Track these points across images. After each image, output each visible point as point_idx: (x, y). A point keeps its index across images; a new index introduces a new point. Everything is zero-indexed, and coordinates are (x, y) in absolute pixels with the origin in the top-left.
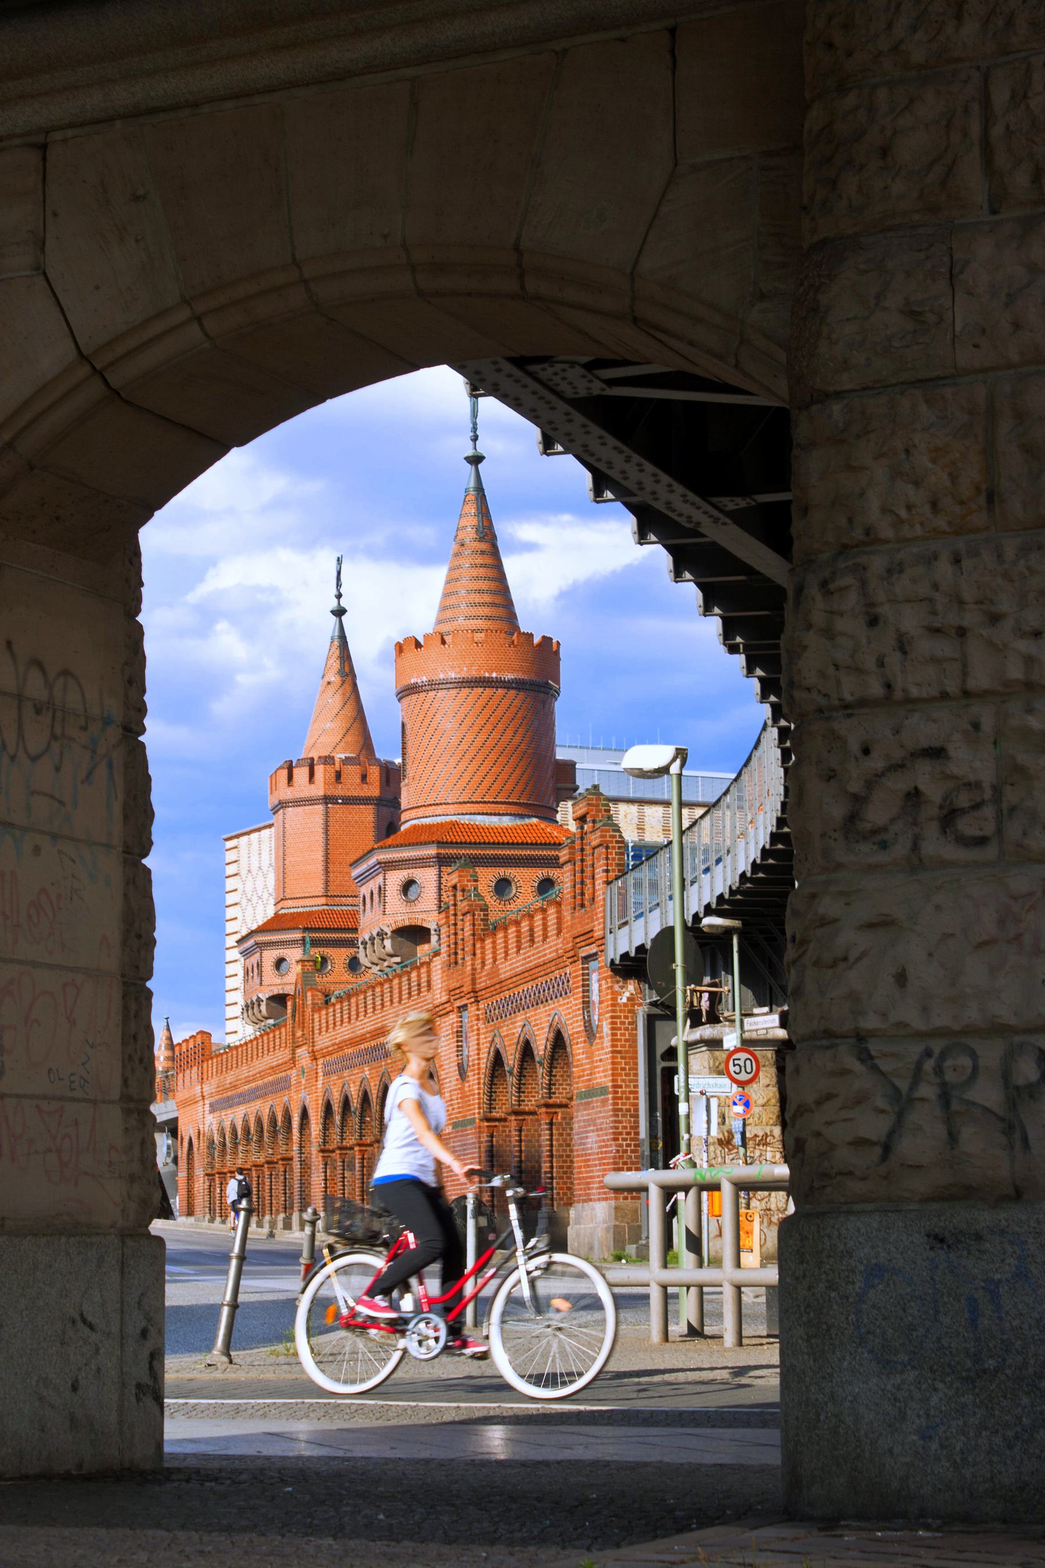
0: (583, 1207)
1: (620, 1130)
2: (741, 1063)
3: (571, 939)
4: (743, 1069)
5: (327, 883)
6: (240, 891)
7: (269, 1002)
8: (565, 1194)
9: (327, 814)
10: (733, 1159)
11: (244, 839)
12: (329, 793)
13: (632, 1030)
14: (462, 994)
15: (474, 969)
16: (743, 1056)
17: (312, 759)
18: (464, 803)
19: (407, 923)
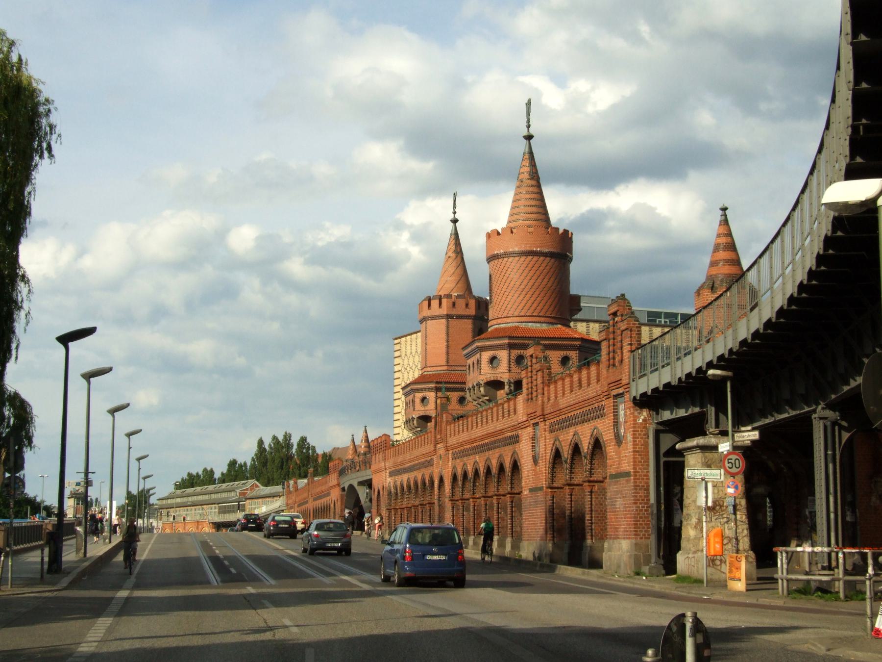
0: (613, 542)
1: (638, 498)
2: (733, 461)
3: (607, 385)
4: (734, 465)
5: (448, 359)
6: (401, 365)
7: (420, 421)
8: (599, 533)
9: (448, 324)
10: (717, 519)
11: (403, 339)
12: (449, 313)
13: (645, 438)
14: (536, 417)
15: (543, 402)
16: (734, 457)
17: (441, 296)
18: (522, 316)
19: (492, 379)
